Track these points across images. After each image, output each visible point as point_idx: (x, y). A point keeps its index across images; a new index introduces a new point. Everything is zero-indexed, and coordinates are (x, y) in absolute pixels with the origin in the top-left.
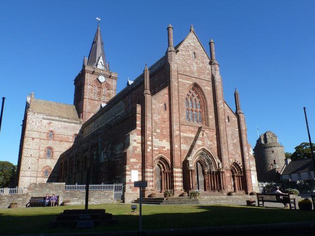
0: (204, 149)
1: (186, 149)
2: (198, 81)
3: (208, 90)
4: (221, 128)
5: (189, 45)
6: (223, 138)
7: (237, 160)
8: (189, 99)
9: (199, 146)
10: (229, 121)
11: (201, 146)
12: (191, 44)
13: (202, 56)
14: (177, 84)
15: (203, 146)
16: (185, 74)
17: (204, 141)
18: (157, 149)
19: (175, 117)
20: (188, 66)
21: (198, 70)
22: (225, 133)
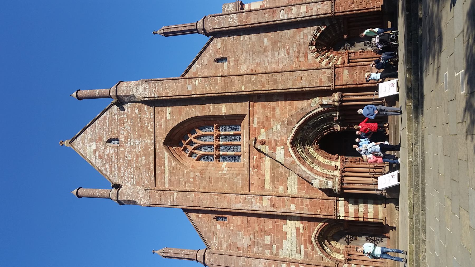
0: (293, 142)
2: (161, 139)
3: (172, 113)
4: (243, 89)
5: (97, 152)
6: (263, 85)
8: (200, 152)
9: (287, 154)
10: (225, 59)
12: (95, 148)
13: (111, 124)
14: (176, 194)
15: (286, 144)
16: (152, 167)
17: (275, 141)
18: (302, 247)
19: (239, 206)
20: (137, 159)
21: (139, 136)
22: (254, 77)
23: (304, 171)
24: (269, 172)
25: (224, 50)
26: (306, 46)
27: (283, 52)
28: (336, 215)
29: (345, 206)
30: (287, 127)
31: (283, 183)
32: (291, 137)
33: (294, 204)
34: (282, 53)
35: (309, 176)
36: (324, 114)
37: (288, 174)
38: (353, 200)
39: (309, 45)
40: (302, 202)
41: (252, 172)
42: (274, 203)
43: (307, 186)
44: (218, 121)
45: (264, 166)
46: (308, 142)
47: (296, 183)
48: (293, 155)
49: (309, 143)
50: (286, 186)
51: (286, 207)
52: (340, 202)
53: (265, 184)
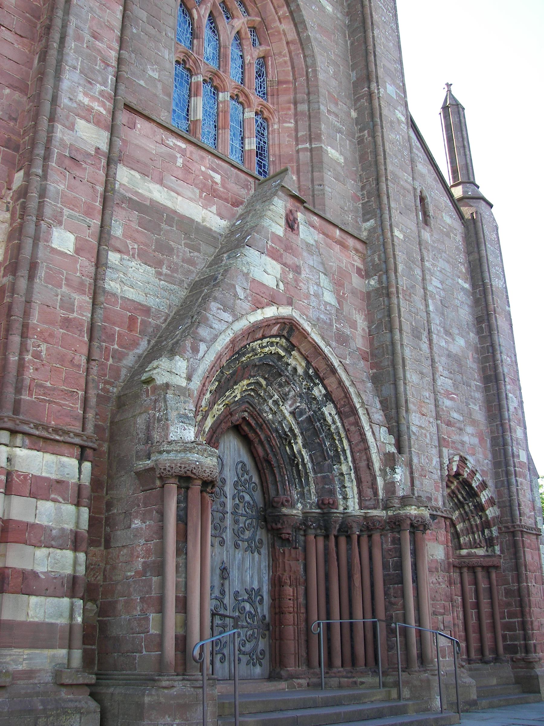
1: (152, 302)
7: (471, 462)
11: (273, 301)
17: (297, 270)
23: (215, 338)
24: (169, 204)
25: (442, 228)
26: (459, 447)
27: (446, 379)
28: (26, 428)
29: (58, 482)
30: (331, 325)
31: (135, 240)
32: (307, 327)
33: (78, 251)
34: (445, 377)
35: (201, 354)
36: (351, 464)
37: (166, 275)
38: (84, 525)
39: (461, 457)
40: (80, 289)
41: (171, 144)
42: (84, 166)
43: (120, 335)
44: (292, 121)
45: (190, 195)
46: (261, 385)
47: (131, 294)
48: (258, 316)
49: (252, 394)
50: (123, 249)
51: (66, 212)
52: (75, 462)
53: (133, 172)
